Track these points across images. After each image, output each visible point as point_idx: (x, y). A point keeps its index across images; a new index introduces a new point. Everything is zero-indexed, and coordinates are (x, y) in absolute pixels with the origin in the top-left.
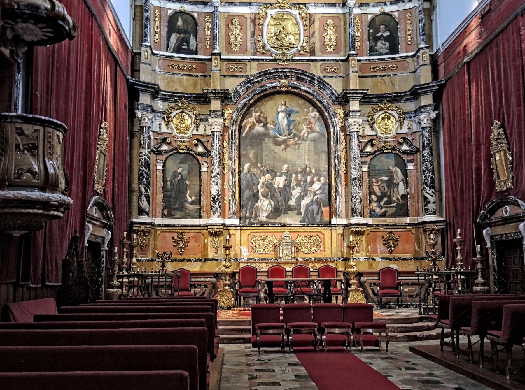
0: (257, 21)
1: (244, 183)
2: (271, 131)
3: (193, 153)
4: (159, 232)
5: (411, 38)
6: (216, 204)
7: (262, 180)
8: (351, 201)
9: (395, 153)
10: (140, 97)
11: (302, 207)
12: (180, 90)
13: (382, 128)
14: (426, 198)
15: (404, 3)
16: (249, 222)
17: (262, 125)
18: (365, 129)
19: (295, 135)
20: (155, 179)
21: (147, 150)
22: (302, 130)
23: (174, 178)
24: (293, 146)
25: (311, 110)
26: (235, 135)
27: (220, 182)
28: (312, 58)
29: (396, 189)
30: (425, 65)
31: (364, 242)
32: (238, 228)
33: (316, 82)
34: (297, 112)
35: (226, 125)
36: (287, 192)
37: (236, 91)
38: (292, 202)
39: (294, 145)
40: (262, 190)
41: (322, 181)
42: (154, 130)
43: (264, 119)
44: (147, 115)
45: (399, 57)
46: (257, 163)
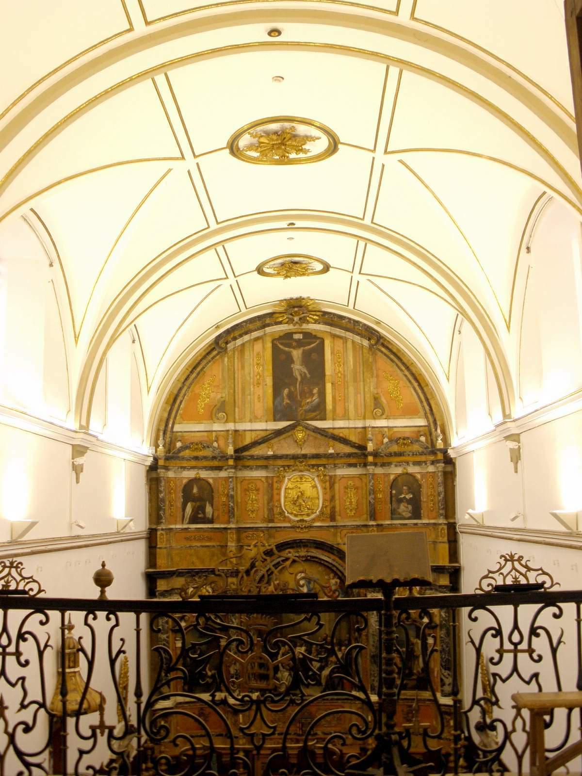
0: (275, 485)
5: (433, 504)
10: (158, 584)
14: (442, 680)
15: (426, 466)
25: (331, 577)
28: (332, 524)
29: (416, 662)
30: (443, 542)
45: (421, 524)
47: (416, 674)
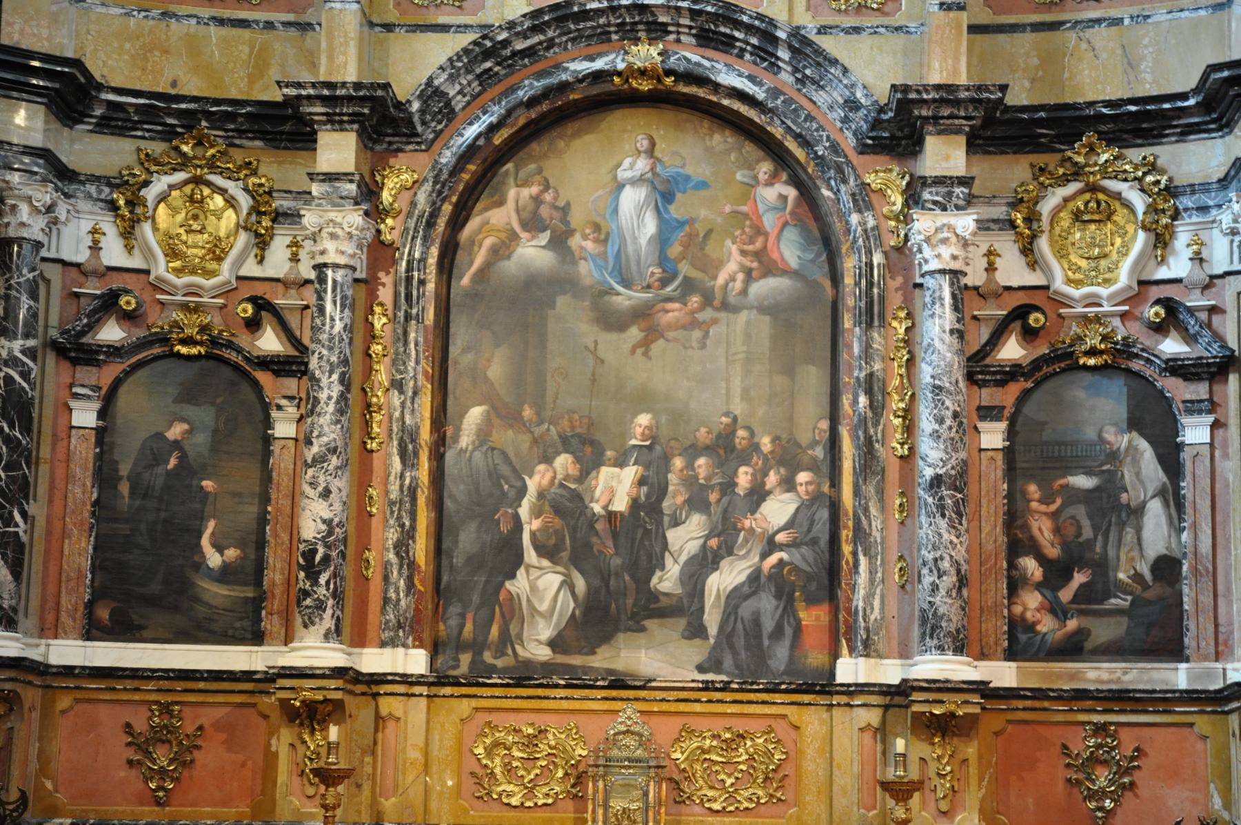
1: (456, 490)
2: (587, 271)
3: (240, 360)
4: (64, 702)
6: (315, 582)
7: (537, 478)
8: (920, 581)
9: (1128, 371)
11: (709, 600)
12: (192, 86)
13: (1073, 258)
16: (473, 663)
17: (544, 238)
18: (999, 263)
19: (689, 286)
20: (60, 472)
21: (17, 345)
22: (720, 264)
23: (151, 466)
24: (679, 334)
25: (762, 177)
26: (422, 282)
27: (340, 484)
29: (1129, 534)
31: (973, 770)
32: (417, 690)
33: (784, 54)
34: (703, 185)
35: (387, 237)
36: (647, 532)
37: (431, 93)
38: (667, 580)
39: (684, 327)
40: (536, 524)
41: (801, 489)
42: (67, 256)
43: (556, 214)
44: (28, 191)
46: (521, 405)
47: (1122, 588)
